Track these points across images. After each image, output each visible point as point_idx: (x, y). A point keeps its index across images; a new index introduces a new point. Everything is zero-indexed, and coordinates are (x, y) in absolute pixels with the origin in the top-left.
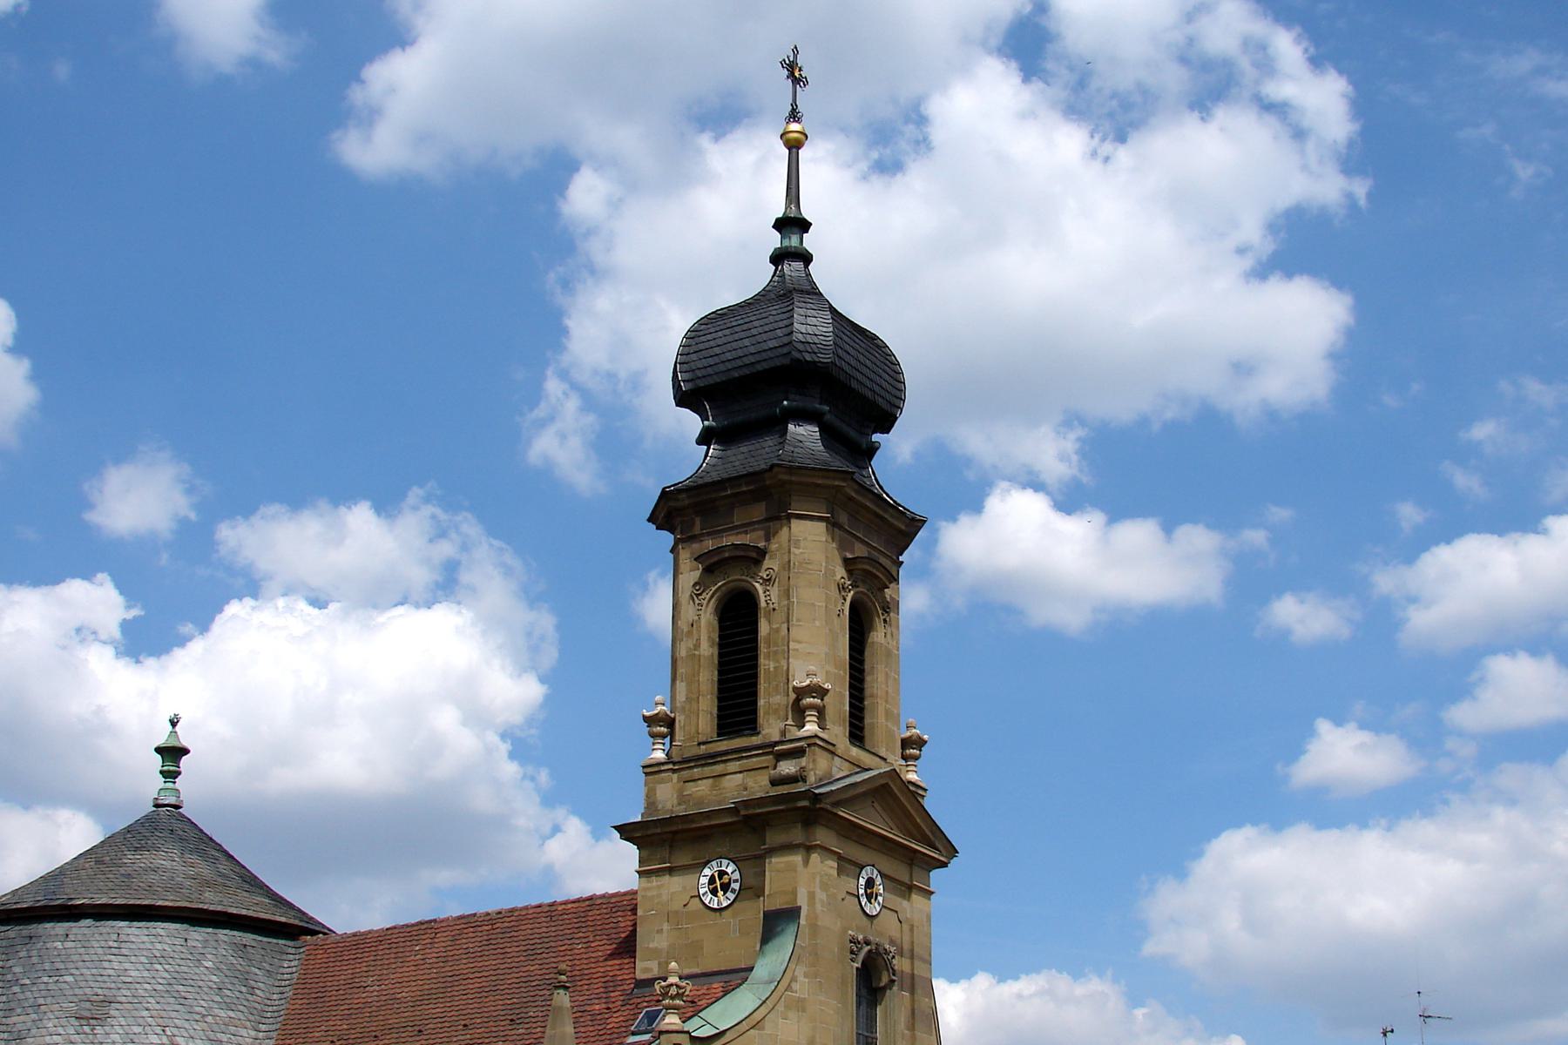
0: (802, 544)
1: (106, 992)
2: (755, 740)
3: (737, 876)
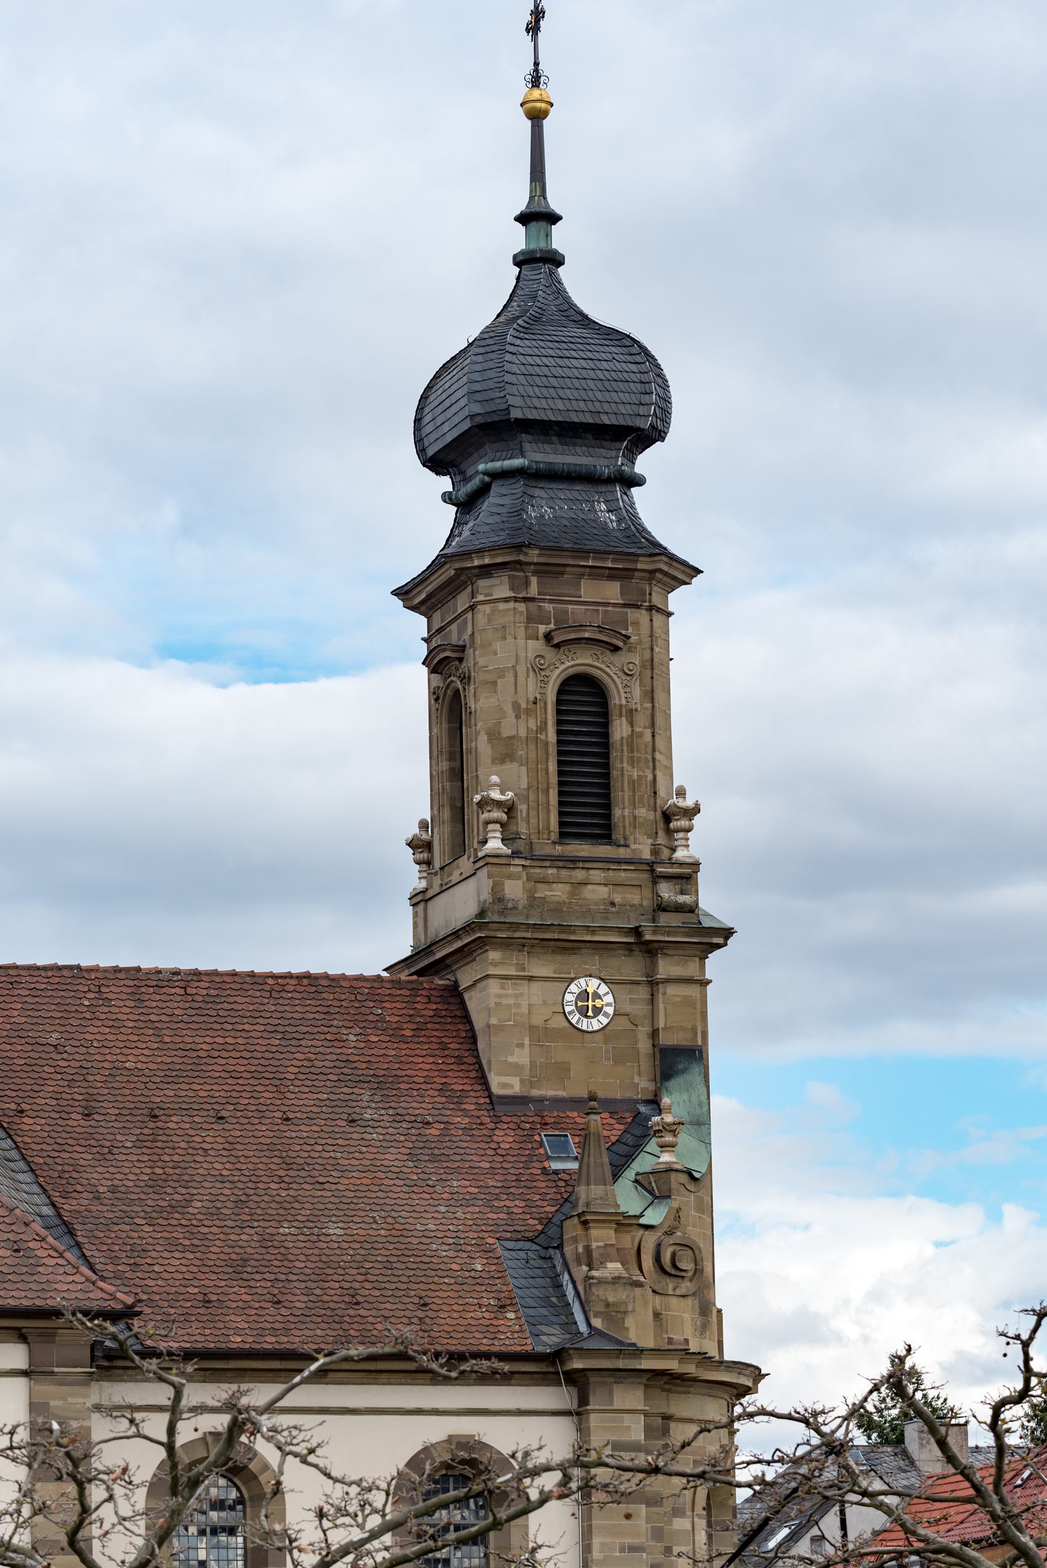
3: (609, 999)
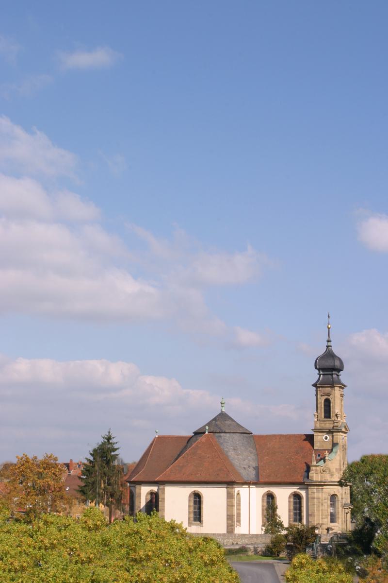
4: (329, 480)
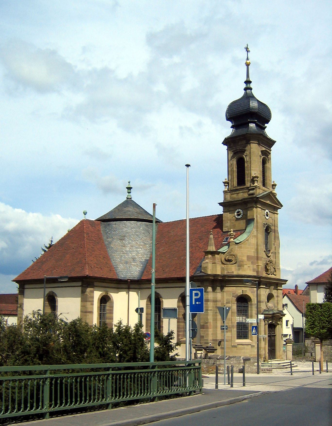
0: (253, 148)
1: (124, 234)
2: (245, 187)
3: (242, 212)
4: (235, 273)
